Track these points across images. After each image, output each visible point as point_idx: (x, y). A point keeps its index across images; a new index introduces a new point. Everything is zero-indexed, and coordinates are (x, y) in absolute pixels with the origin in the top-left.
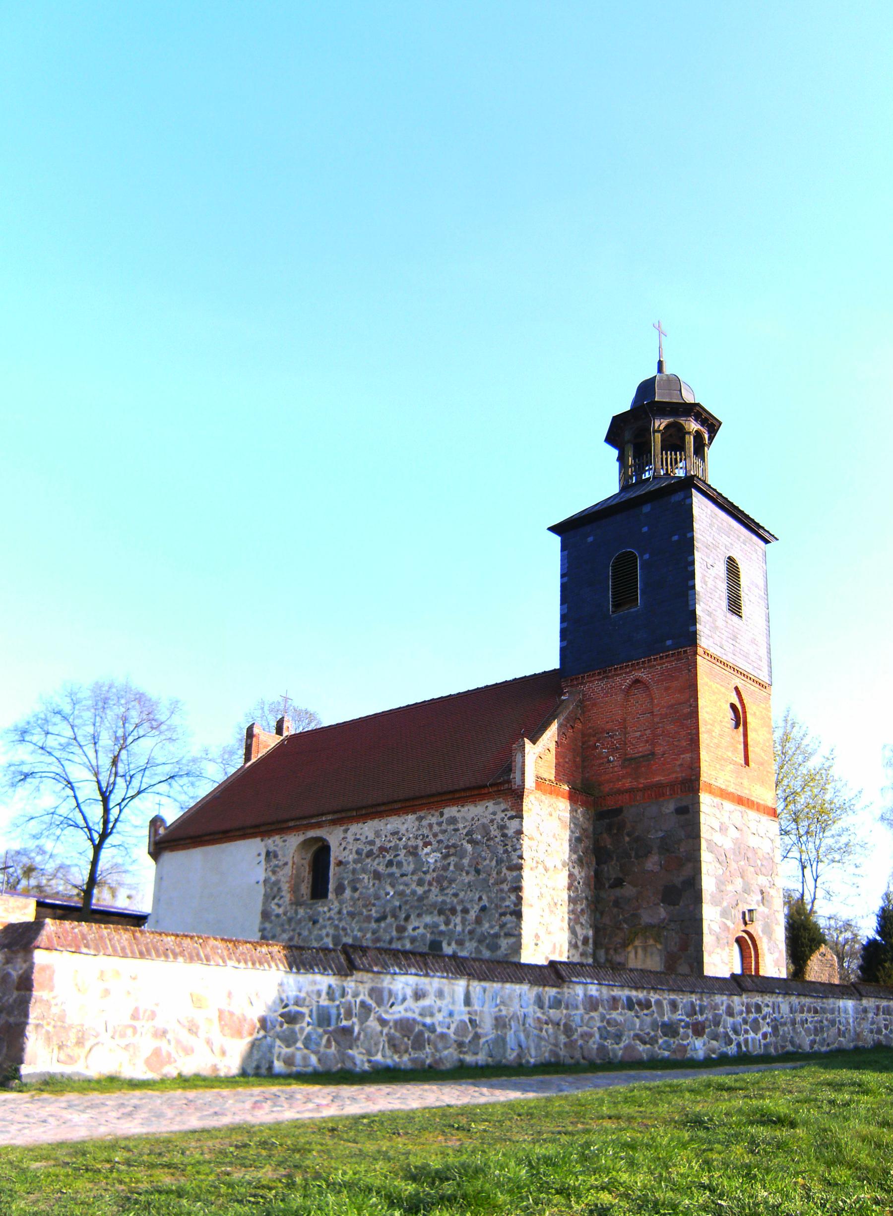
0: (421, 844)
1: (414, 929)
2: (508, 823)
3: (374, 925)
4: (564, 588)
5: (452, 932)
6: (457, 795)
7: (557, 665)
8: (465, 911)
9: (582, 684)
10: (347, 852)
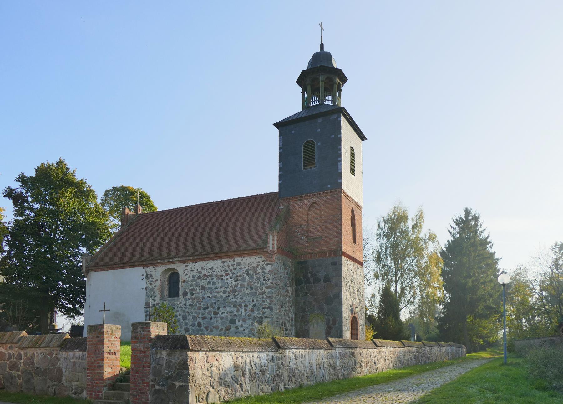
0: (224, 274)
1: (222, 313)
2: (266, 267)
3: (202, 311)
4: (280, 154)
5: (240, 315)
6: (242, 253)
7: (276, 189)
8: (246, 306)
9: (289, 202)
10: (188, 276)
